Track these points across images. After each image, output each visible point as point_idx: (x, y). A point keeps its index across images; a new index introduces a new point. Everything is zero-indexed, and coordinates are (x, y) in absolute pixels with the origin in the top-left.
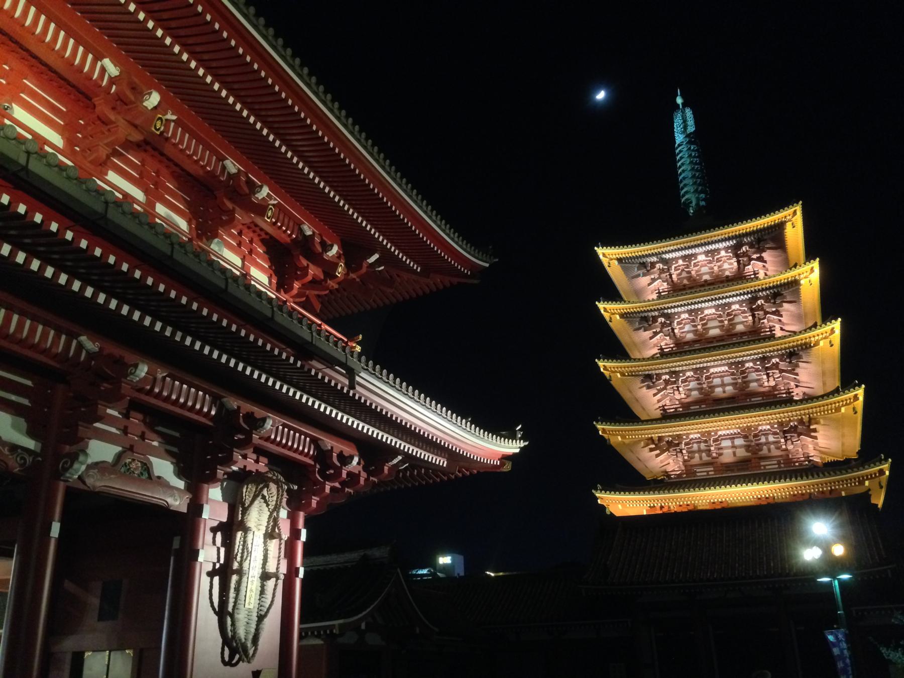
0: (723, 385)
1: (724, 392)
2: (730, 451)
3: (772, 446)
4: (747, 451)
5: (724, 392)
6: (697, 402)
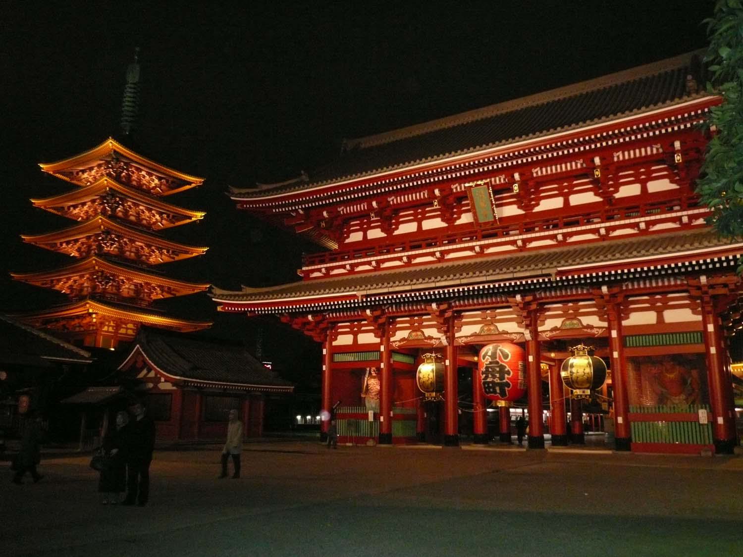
0: (131, 252)
1: (130, 255)
2: (126, 290)
3: (145, 295)
4: (134, 293)
5: (130, 255)
6: (116, 256)
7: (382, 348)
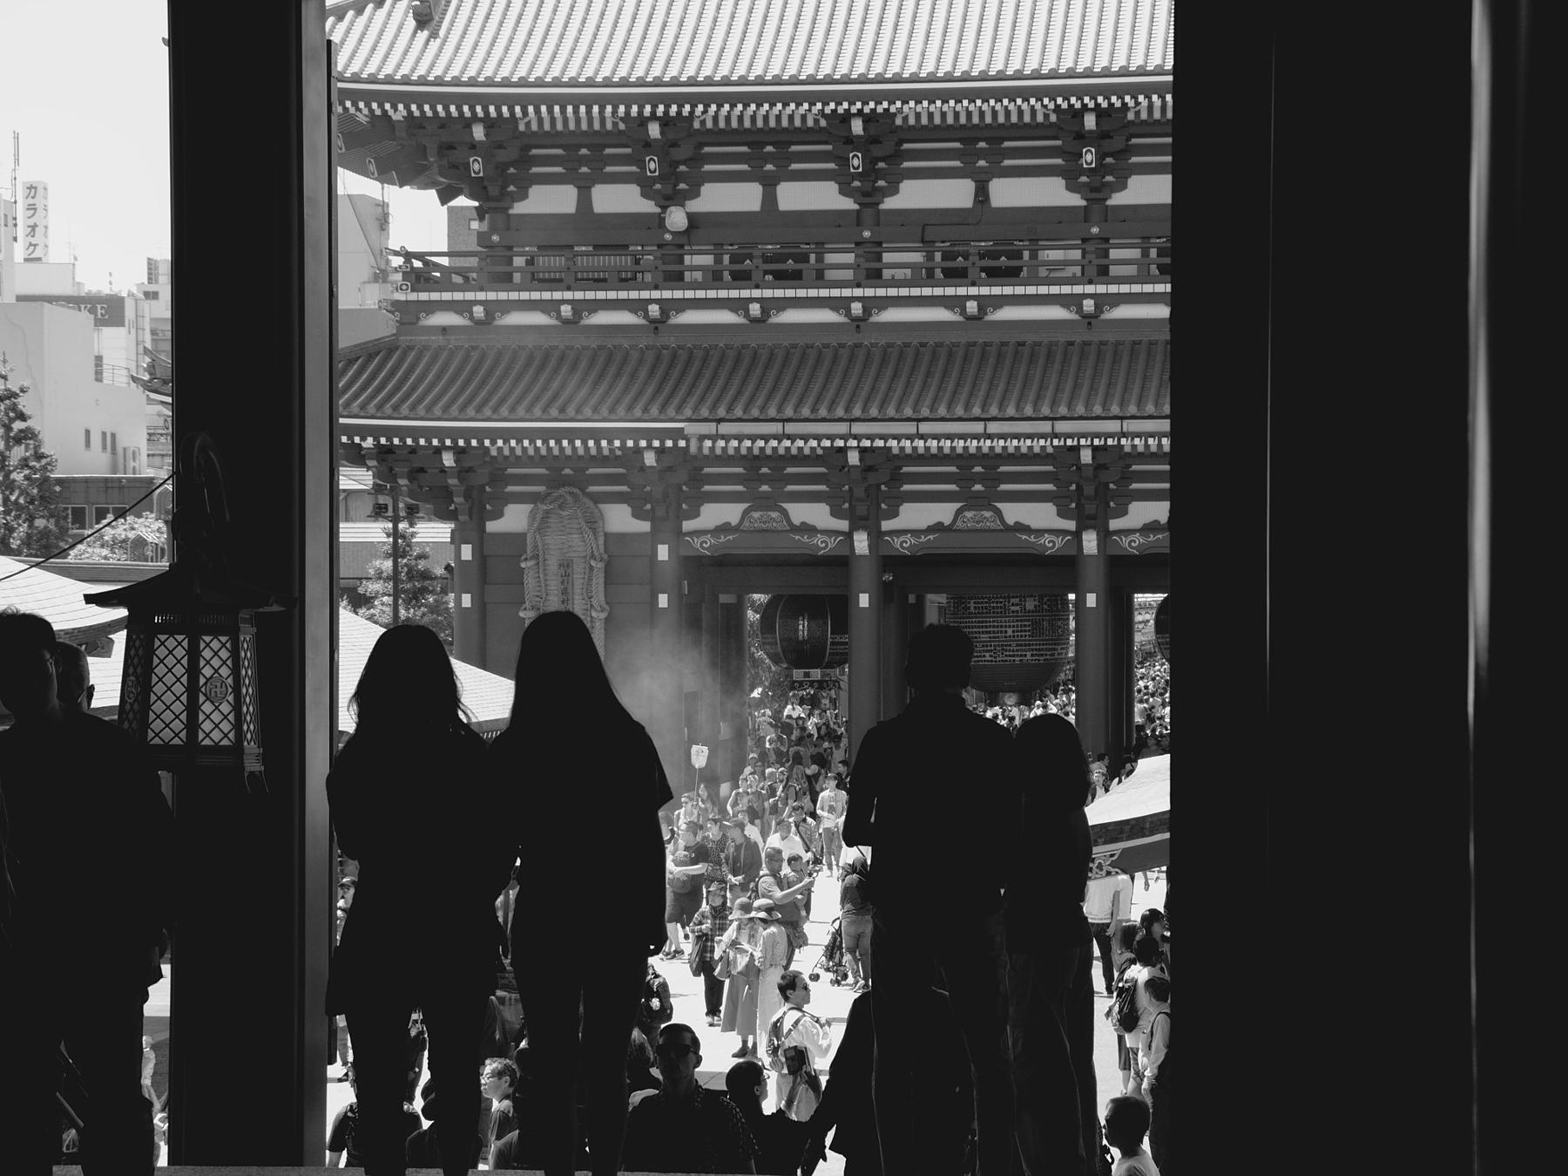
7: (663, 552)
